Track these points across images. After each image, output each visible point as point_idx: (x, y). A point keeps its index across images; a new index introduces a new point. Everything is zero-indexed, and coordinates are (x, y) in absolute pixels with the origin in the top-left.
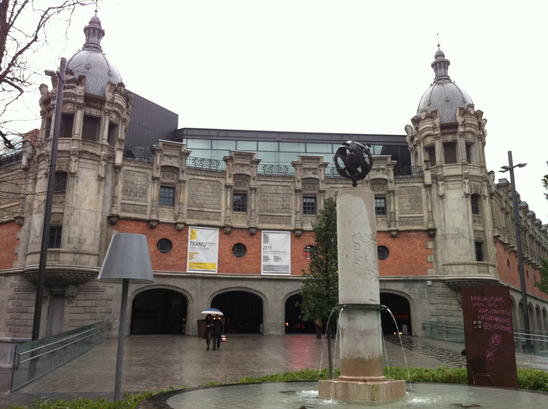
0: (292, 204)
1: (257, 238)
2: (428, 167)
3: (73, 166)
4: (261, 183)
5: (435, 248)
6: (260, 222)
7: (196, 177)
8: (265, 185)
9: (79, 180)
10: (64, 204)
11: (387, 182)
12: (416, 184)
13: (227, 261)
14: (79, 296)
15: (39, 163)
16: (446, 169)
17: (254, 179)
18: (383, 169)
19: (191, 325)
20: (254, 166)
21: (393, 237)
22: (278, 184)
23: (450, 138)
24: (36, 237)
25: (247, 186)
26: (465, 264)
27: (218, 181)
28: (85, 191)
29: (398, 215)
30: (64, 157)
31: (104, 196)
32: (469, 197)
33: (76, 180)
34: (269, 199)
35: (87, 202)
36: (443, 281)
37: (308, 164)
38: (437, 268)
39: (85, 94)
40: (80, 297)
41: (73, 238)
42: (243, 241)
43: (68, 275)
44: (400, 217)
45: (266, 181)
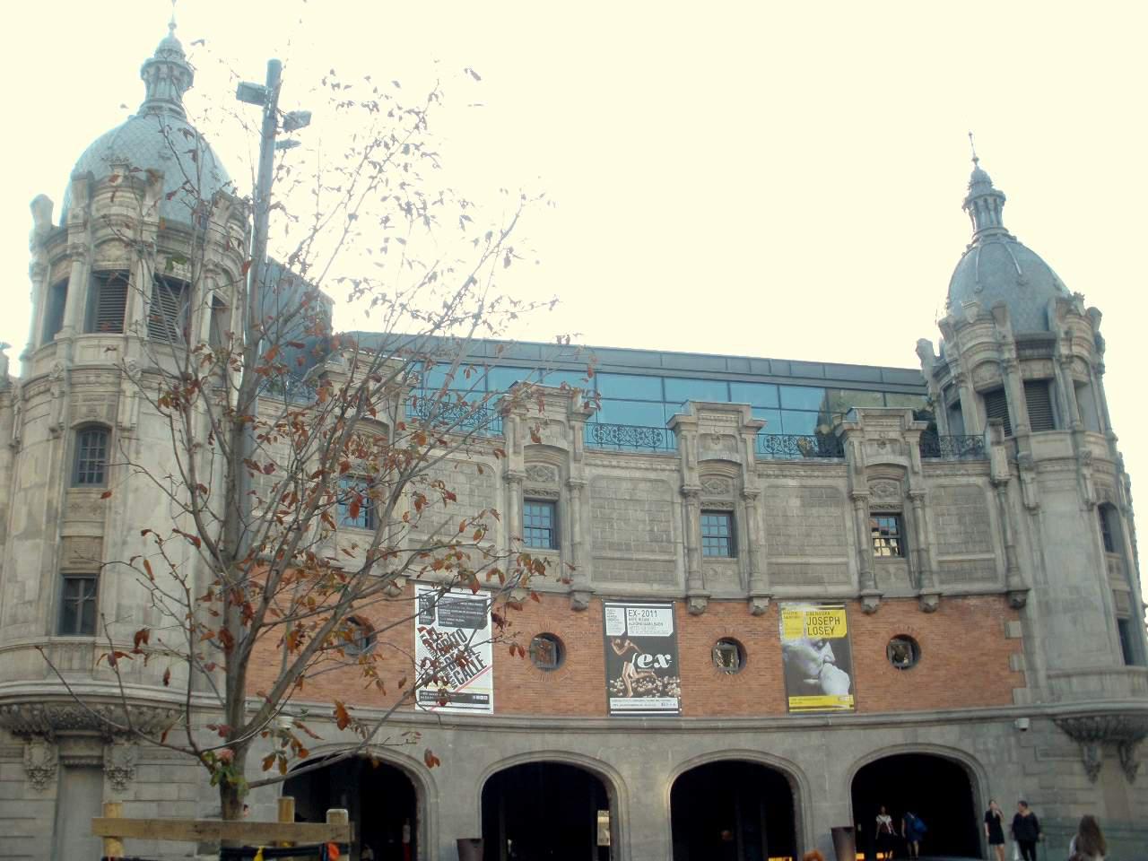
0: (675, 529)
1: (591, 619)
2: (999, 436)
3: (128, 408)
5: (1027, 637)
6: (594, 579)
8: (608, 478)
9: (142, 449)
10: (104, 513)
11: (906, 474)
12: (973, 480)
13: (516, 680)
14: (143, 770)
15: (26, 400)
16: (1039, 442)
17: (576, 460)
18: (893, 441)
19: (434, 853)
20: (577, 424)
21: (927, 610)
22: (638, 474)
23: (1038, 370)
24: (24, 603)
25: (557, 479)
26: (1101, 673)
29: (934, 558)
30: (102, 384)
32: (1096, 508)
33: (133, 449)
34: (615, 516)
36: (1052, 717)
37: (710, 423)
38: (1036, 686)
39: (163, 220)
40: (146, 773)
41: (131, 608)
42: (556, 629)
43: (119, 712)
44: (940, 562)
45: (604, 466)
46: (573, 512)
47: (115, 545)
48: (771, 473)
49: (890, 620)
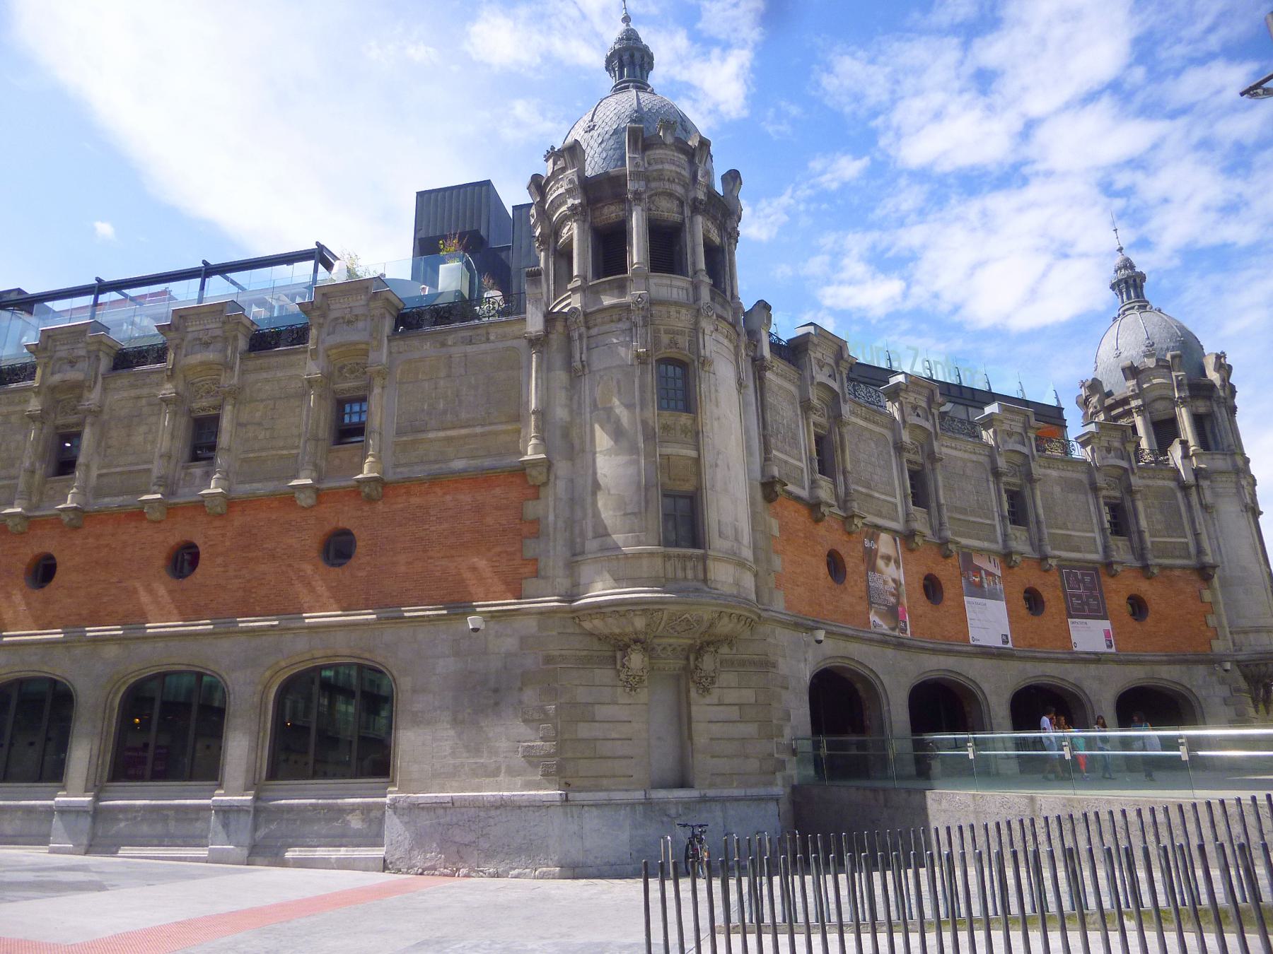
23: (1202, 407)
45: (952, 448)
46: (936, 481)
49: (1127, 583)
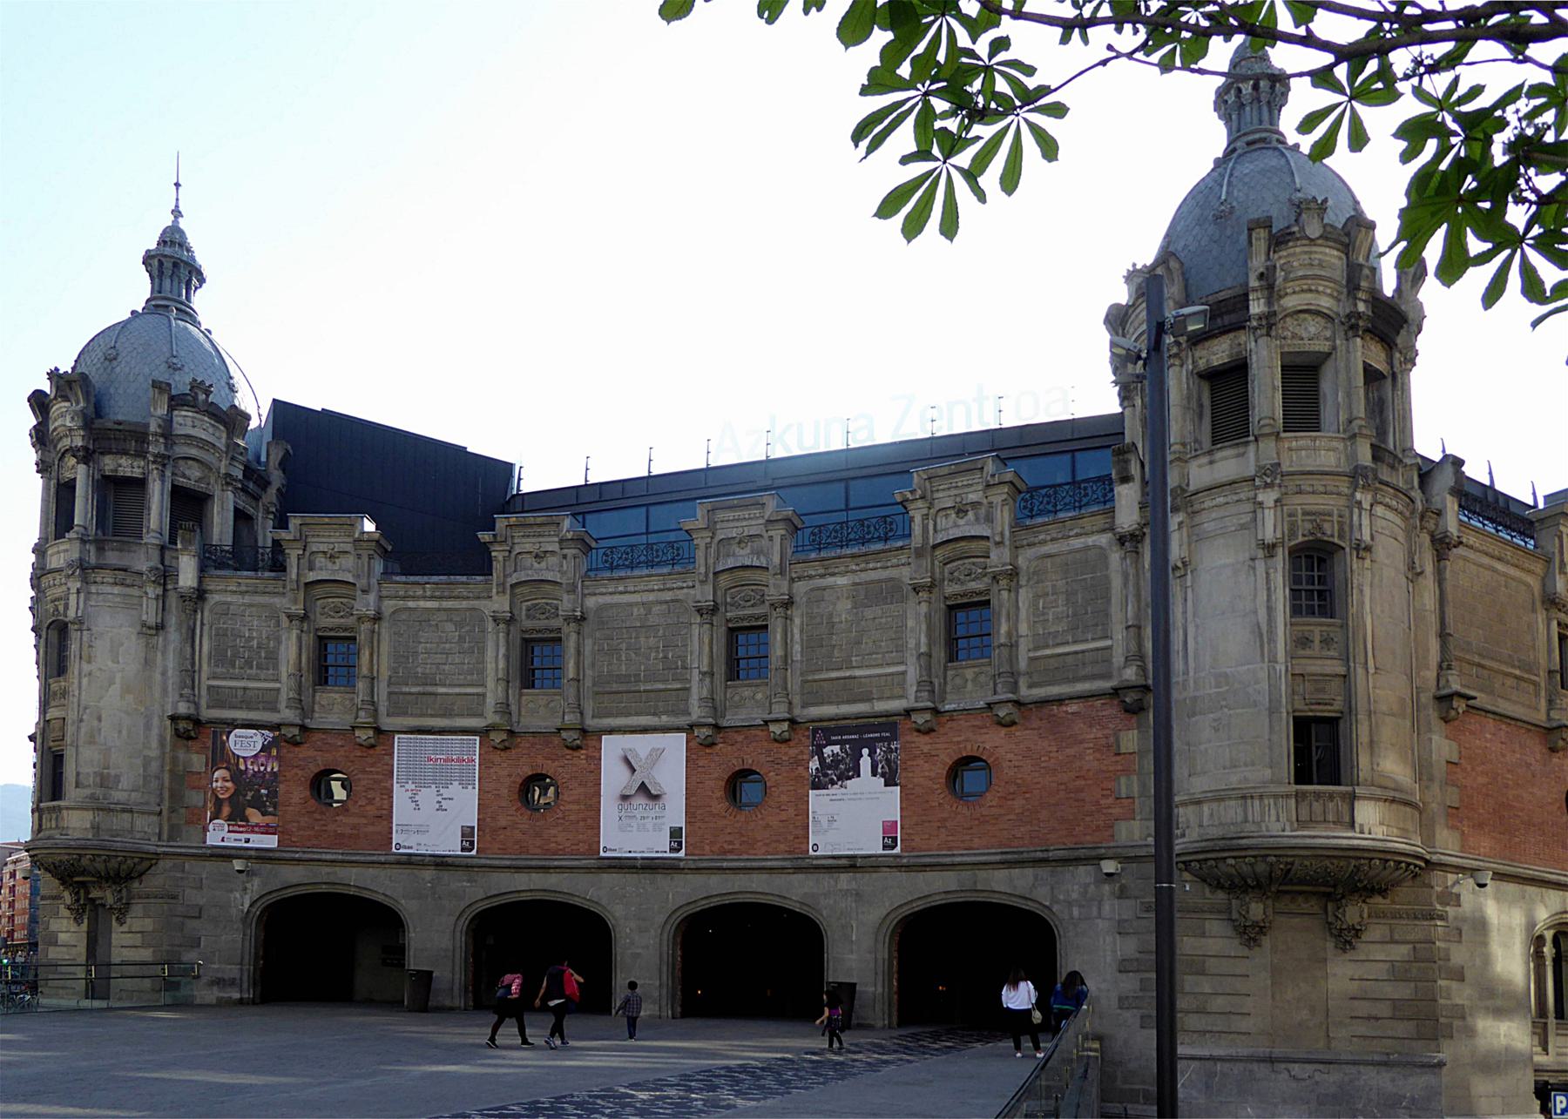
4: (601, 600)
7: (411, 604)
8: (612, 606)
22: (651, 597)
27: (475, 609)
28: (110, 663)
31: (164, 673)
35: (115, 689)
37: (731, 524)
44: (1032, 659)
45: (611, 594)
47: (73, 722)
48: (813, 573)
49: (955, 739)
